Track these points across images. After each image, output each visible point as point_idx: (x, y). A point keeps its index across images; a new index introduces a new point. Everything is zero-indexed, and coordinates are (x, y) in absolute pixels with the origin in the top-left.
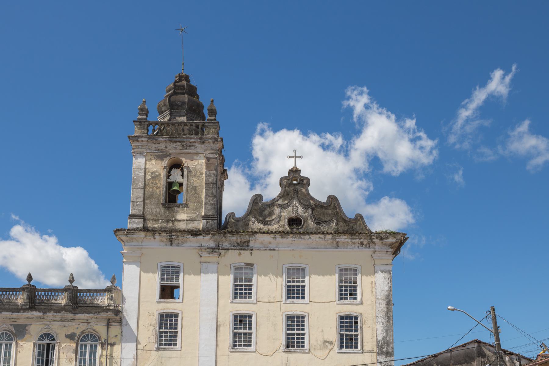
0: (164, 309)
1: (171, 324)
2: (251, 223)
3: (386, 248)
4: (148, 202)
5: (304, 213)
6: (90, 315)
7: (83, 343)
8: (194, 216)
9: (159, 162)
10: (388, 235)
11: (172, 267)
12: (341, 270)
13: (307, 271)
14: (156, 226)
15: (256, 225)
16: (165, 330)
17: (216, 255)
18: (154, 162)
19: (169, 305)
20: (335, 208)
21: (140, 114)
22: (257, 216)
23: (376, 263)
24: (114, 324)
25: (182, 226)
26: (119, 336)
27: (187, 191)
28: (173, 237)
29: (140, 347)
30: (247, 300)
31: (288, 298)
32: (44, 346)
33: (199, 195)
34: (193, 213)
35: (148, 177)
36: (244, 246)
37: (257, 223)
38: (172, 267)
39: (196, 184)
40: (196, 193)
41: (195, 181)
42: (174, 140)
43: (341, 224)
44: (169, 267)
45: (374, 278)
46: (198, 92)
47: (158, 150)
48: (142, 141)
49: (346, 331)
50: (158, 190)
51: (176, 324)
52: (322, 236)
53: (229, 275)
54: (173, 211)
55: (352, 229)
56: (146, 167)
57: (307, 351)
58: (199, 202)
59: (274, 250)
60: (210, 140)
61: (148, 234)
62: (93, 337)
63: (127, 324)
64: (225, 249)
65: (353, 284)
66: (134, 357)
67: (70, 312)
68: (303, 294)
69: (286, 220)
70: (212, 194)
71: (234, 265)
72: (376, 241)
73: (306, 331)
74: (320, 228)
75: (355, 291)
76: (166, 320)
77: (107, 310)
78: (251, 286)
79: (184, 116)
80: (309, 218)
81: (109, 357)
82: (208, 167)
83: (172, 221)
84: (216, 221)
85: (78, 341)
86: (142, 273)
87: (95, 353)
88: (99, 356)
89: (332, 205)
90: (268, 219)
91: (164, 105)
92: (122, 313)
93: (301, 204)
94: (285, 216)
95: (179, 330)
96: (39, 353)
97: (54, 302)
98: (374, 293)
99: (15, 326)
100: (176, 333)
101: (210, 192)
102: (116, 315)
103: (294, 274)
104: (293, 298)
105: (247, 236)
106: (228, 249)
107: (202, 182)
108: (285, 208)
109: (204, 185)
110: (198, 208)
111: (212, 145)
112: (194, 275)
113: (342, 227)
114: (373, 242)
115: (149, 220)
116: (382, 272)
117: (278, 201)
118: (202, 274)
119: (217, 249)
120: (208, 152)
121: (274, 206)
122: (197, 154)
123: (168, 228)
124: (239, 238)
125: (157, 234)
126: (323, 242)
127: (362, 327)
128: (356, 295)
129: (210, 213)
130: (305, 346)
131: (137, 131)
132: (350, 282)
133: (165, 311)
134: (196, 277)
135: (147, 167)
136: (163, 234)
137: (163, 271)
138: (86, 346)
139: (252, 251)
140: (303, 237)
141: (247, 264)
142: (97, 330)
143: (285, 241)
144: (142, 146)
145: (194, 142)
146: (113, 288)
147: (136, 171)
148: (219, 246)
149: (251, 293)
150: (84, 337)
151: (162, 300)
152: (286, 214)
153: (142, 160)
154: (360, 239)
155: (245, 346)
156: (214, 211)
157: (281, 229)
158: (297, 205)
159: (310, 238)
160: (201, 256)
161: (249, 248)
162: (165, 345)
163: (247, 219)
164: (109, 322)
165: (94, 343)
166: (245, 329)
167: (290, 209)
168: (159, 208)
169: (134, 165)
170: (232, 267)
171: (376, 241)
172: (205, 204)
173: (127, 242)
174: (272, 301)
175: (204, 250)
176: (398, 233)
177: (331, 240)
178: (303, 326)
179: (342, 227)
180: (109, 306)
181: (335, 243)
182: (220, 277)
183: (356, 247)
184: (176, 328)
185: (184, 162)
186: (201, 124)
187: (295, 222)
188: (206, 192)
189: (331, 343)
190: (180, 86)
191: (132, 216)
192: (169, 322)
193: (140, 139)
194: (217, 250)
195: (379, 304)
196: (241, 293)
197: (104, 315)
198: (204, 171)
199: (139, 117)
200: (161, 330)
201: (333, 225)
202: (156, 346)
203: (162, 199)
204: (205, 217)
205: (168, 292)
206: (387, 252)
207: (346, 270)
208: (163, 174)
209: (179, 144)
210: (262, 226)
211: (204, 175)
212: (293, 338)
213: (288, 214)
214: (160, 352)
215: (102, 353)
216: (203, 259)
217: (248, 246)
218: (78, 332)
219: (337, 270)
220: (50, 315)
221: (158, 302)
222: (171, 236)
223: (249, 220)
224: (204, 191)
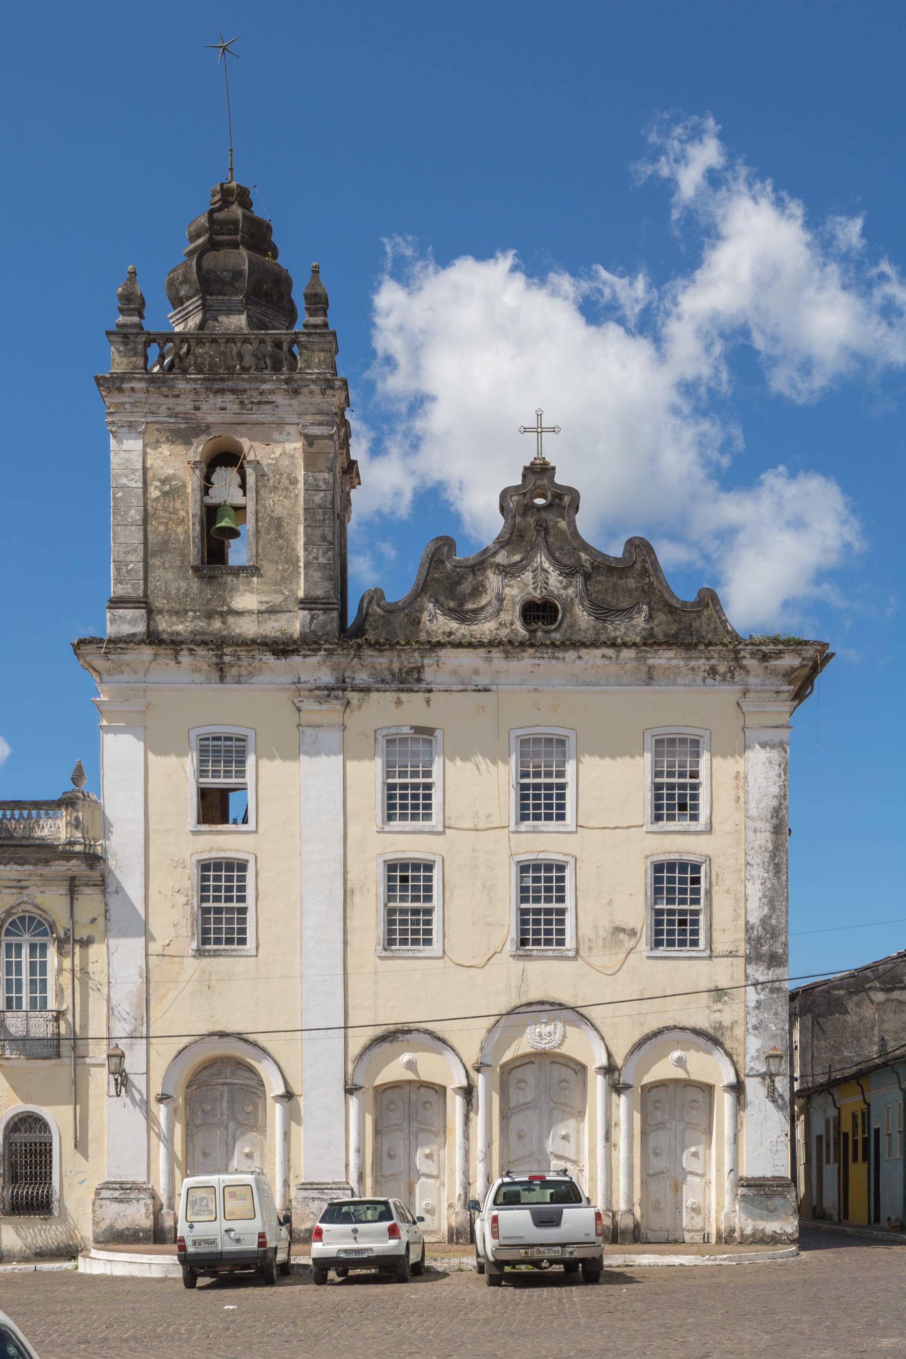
0: (211, 850)
2: (425, 617)
3: (775, 680)
4: (155, 561)
5: (565, 588)
6: (26, 867)
7: (13, 940)
8: (278, 599)
9: (180, 449)
10: (781, 647)
11: (226, 739)
12: (659, 743)
13: (571, 746)
14: (180, 628)
15: (437, 623)
16: (216, 905)
17: (337, 706)
18: (165, 449)
19: (221, 840)
20: (644, 573)
21: (122, 311)
22: (442, 599)
23: (750, 721)
24: (88, 890)
25: (247, 628)
26: (101, 921)
27: (258, 531)
28: (227, 659)
29: (154, 947)
30: (420, 824)
31: (524, 818)
33: (287, 540)
34: (276, 592)
35: (154, 493)
36: (408, 680)
37: (441, 618)
38: (226, 739)
39: (279, 511)
40: (280, 537)
41: (277, 504)
42: (217, 386)
43: (661, 617)
44: (219, 739)
45: (742, 761)
46: (276, 238)
47: (176, 415)
48: (133, 389)
49: (670, 901)
50: (180, 529)
51: (242, 889)
52: (610, 652)
53: (372, 758)
54: (223, 586)
55: (690, 631)
56: (146, 462)
57: (571, 954)
58: (288, 561)
59: (486, 690)
60: (312, 387)
61: (161, 651)
62: (36, 924)
63: (119, 890)
64: (361, 690)
65: (688, 780)
66: (140, 973)
68: (562, 807)
69: (518, 608)
70: (324, 538)
71: (384, 732)
72: (750, 663)
73: (569, 903)
74: (605, 628)
75: (695, 797)
76: (217, 878)
77: (68, 856)
78: (428, 786)
79: (240, 312)
80: (577, 601)
81: (78, 974)
82: (310, 463)
83: (221, 614)
84: (335, 614)
86: (151, 755)
87: (44, 965)
88: (55, 972)
89: (638, 566)
90: (470, 606)
91: (186, 281)
93: (557, 562)
94: (514, 597)
95: (250, 903)
98: (742, 801)
100: (243, 911)
101: (318, 532)
102: (92, 867)
103: (537, 754)
104: (537, 817)
105: (416, 654)
106: (367, 690)
107: (294, 505)
108: (513, 576)
109: (301, 512)
110: (288, 579)
111: (318, 399)
113: (663, 624)
114: (742, 667)
115: (160, 612)
116: (763, 746)
117: (494, 554)
118: (302, 757)
119: (338, 690)
120: (309, 419)
121: (485, 570)
122: (280, 425)
123: (211, 633)
124: (395, 660)
125: (185, 652)
126: (613, 668)
127: (709, 892)
128: (695, 807)
129: (319, 592)
130: (567, 942)
131: (118, 362)
132: (682, 775)
133: (213, 855)
134: (289, 766)
135: (149, 463)
136: (201, 651)
137: (203, 751)
138: (19, 947)
139: (431, 695)
140: (560, 655)
141: (419, 730)
142: (44, 906)
143: (513, 665)
144: (134, 404)
145: (272, 392)
146: (79, 798)
147: (120, 476)
148: (344, 681)
149: (428, 807)
150: (13, 923)
151: (205, 827)
152: (516, 591)
153: (134, 445)
154: (708, 659)
155: (415, 942)
156: (328, 585)
157: (504, 633)
158: (546, 565)
159: (580, 657)
160: (299, 710)
161: (423, 686)
162: (218, 941)
163: (417, 605)
164: (73, 886)
165: (38, 940)
166: (416, 899)
167: (528, 576)
168: (185, 578)
169: (115, 460)
170: (379, 738)
171: (750, 663)
172: (305, 566)
173: (109, 672)
174: (482, 825)
175: (307, 693)
176: (806, 643)
177: (634, 663)
178: (561, 889)
179: (663, 624)
180: (71, 843)
181: (644, 669)
182: (348, 763)
183: (699, 681)
184: (242, 899)
185: (246, 448)
186: (288, 338)
187: (539, 612)
188: (306, 534)
189: (633, 933)
190: (225, 222)
191: (117, 603)
192: (223, 884)
193: (126, 386)
194: (340, 693)
195: (755, 831)
196: (404, 807)
197: (59, 868)
198: (300, 474)
199: (121, 319)
200: (205, 905)
201: (640, 620)
202: (194, 945)
203: (193, 553)
204: (307, 603)
206: (778, 692)
207: (672, 742)
208: (192, 482)
209: (230, 397)
210: (454, 625)
211: (301, 485)
212: (537, 922)
213: (522, 590)
214: (205, 961)
215: (60, 963)
216: (305, 717)
217: (419, 680)
219: (650, 742)
221: (195, 833)
222: (221, 657)
223: (421, 611)
224: (301, 529)
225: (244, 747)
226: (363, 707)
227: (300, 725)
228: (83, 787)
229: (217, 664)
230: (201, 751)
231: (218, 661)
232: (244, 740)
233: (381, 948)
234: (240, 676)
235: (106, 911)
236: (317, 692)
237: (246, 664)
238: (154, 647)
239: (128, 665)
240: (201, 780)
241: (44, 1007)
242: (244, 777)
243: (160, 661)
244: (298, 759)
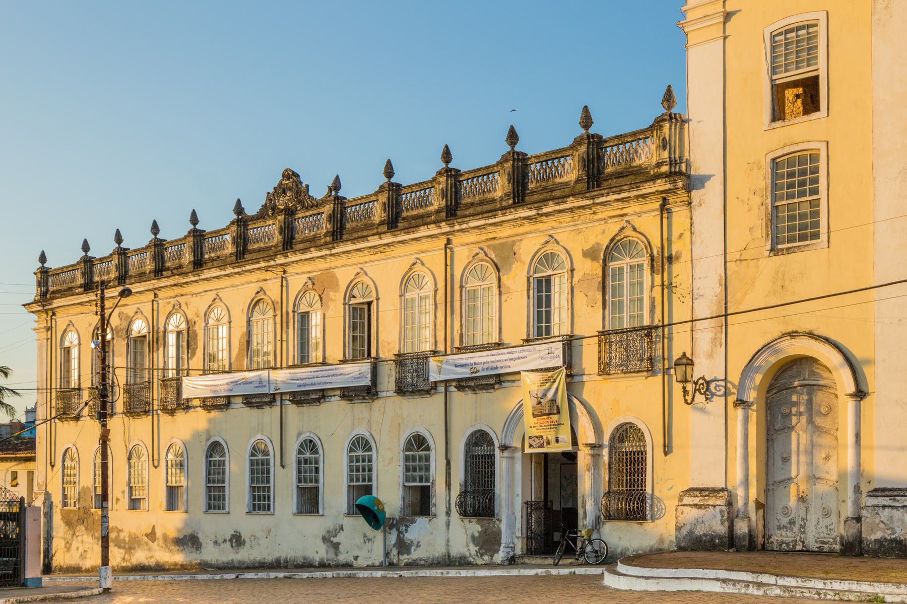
11: (799, 29)
66: (720, 281)
97: (558, 180)
162: (791, 240)
180: (659, 165)
184: (815, 191)
225: (816, 31)
232: (816, 25)
240: (774, 77)
242: (816, 64)
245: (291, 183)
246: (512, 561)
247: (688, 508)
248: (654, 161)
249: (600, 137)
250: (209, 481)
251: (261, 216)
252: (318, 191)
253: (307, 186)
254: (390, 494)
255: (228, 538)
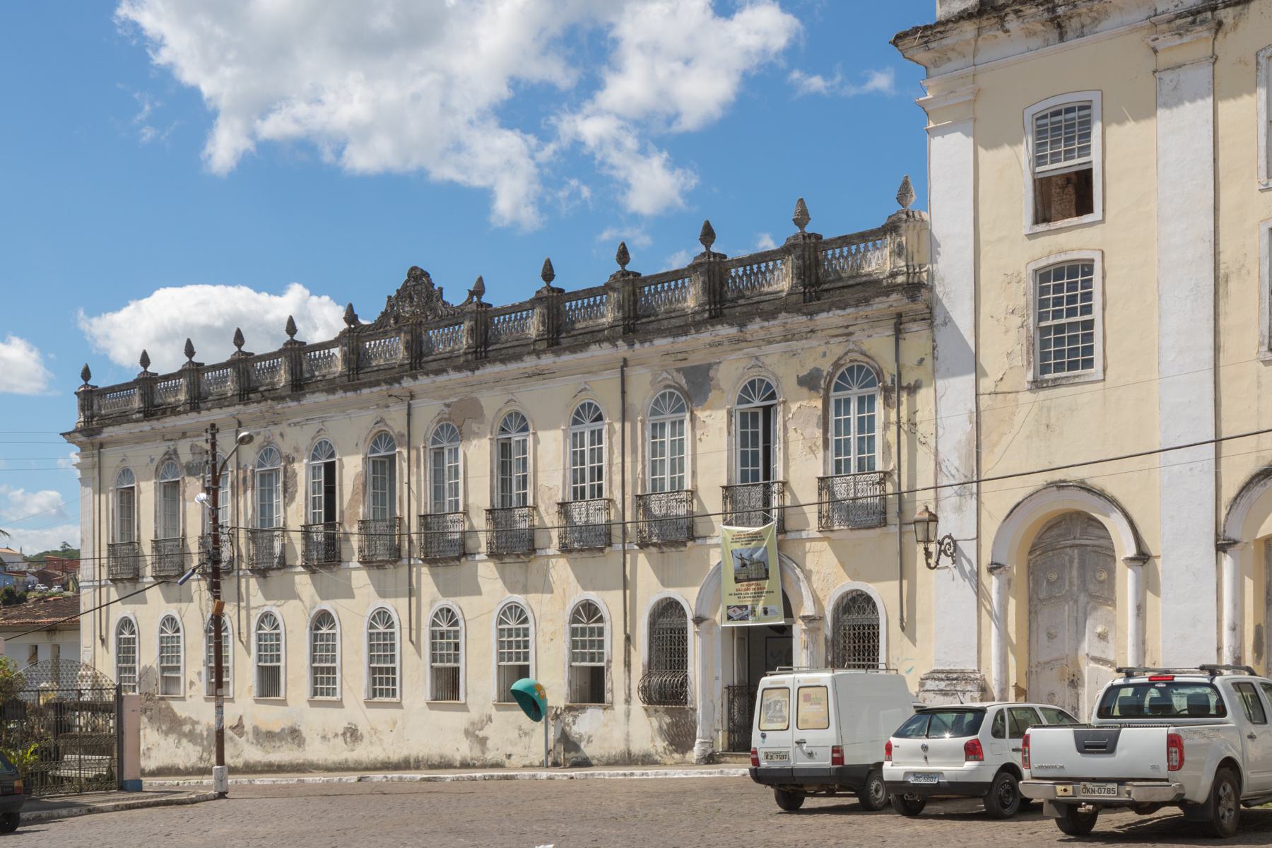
1: (1072, 299)
6: (848, 311)
7: (842, 395)
11: (1068, 111)
17: (1203, 32)
19: (1062, 239)
24: (914, 327)
28: (1060, 11)
29: (986, 384)
32: (755, 416)
38: (1068, 111)
51: (1088, 296)
53: (1252, 91)
61: (985, 23)
62: (857, 373)
63: (948, 321)
67: (799, 311)
76: (1058, 289)
77: (888, 290)
81: (905, 427)
85: (827, 390)
86: (981, 151)
87: (872, 418)
88: (882, 425)
92: (931, 289)
95: (1096, 314)
96: (744, 436)
97: (766, 289)
99: (687, 372)
100: (1089, 325)
102: (913, 299)
112: (1136, 119)
118: (1160, 112)
125: (1011, 16)
133: (1052, 260)
137: (1040, 133)
138: (847, 401)
142: (871, 353)
150: (842, 377)
151: (1043, 227)
160: (1155, 51)
162: (1059, 367)
164: (899, 325)
165: (866, 392)
173: (936, 64)
175: (1165, 27)
180: (893, 275)
182: (1222, 106)
184: (1087, 310)
194: (1209, 14)
197: (880, 305)
200: (1043, 324)
202: (1030, 377)
205: (1067, 195)
214: (1043, 394)
215: (887, 417)
216: (1164, 59)
218: (826, 367)
220: (755, 327)
221: (1031, 236)
222: (1053, 10)
226: (1241, 25)
227: (1155, 72)
228: (910, 207)
229: (1052, 20)
230: (1039, 133)
231: (1051, 15)
232: (1089, 107)
233: (1265, 348)
234: (1083, 27)
235: (934, 348)
236: (1179, 22)
237: (1084, 10)
238: (974, 20)
239: (953, 49)
240: (1038, 169)
241: (872, 470)
242: (1089, 154)
243: (985, 34)
244: (1155, 115)
245: (418, 284)
246: (710, 759)
247: (931, 695)
248: (888, 268)
249: (819, 237)
250: (314, 660)
251: (379, 329)
252: (455, 296)
253: (441, 289)
254: (552, 676)
255: (341, 731)
